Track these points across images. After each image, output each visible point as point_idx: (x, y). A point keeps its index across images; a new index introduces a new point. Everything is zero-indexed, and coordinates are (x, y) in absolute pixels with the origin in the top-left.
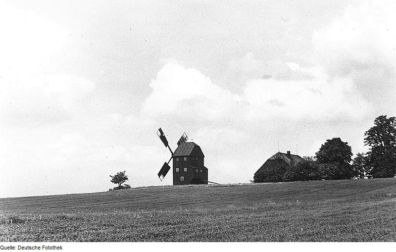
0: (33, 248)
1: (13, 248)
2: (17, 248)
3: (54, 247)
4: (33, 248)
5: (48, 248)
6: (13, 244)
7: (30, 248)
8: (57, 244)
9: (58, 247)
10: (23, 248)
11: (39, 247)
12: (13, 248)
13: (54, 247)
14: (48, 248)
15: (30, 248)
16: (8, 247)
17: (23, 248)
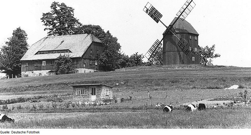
0: (21, 132)
1: (8, 132)
2: (11, 132)
3: (34, 132)
4: (21, 132)
5: (31, 132)
6: (9, 130)
7: (19, 133)
8: (36, 130)
9: (37, 132)
11: (25, 132)
12: (8, 132)
15: (19, 133)
16: (5, 132)
17: (14, 132)
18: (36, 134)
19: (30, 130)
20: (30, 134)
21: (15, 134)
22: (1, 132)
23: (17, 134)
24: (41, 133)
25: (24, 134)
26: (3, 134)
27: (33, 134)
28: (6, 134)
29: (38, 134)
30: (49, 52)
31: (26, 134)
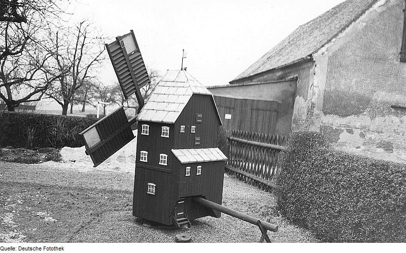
0: (34, 249)
1: (13, 249)
2: (17, 249)
3: (55, 248)
4: (34, 249)
5: (50, 249)
7: (31, 249)
8: (59, 245)
9: (60, 248)
10: (23, 249)
12: (13, 249)
13: (55, 248)
14: (50, 249)
15: (31, 249)
16: (9, 248)
17: (23, 249)
18: (59, 251)
19: (48, 245)
20: (49, 251)
21: (25, 251)
22: (2, 248)
23: (28, 251)
24: (66, 250)
25: (39, 251)
26: (4, 251)
27: (54, 251)
28: (10, 251)
29: (61, 251)
30: (87, 131)
31: (42, 251)
